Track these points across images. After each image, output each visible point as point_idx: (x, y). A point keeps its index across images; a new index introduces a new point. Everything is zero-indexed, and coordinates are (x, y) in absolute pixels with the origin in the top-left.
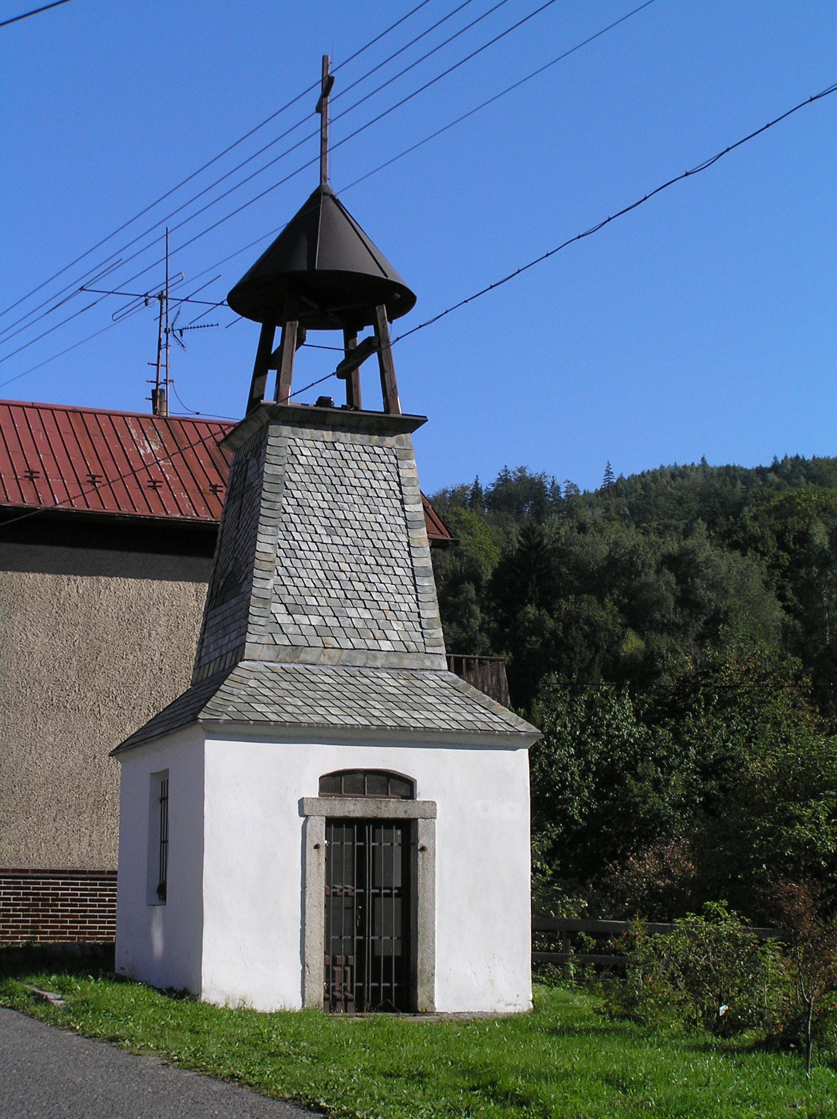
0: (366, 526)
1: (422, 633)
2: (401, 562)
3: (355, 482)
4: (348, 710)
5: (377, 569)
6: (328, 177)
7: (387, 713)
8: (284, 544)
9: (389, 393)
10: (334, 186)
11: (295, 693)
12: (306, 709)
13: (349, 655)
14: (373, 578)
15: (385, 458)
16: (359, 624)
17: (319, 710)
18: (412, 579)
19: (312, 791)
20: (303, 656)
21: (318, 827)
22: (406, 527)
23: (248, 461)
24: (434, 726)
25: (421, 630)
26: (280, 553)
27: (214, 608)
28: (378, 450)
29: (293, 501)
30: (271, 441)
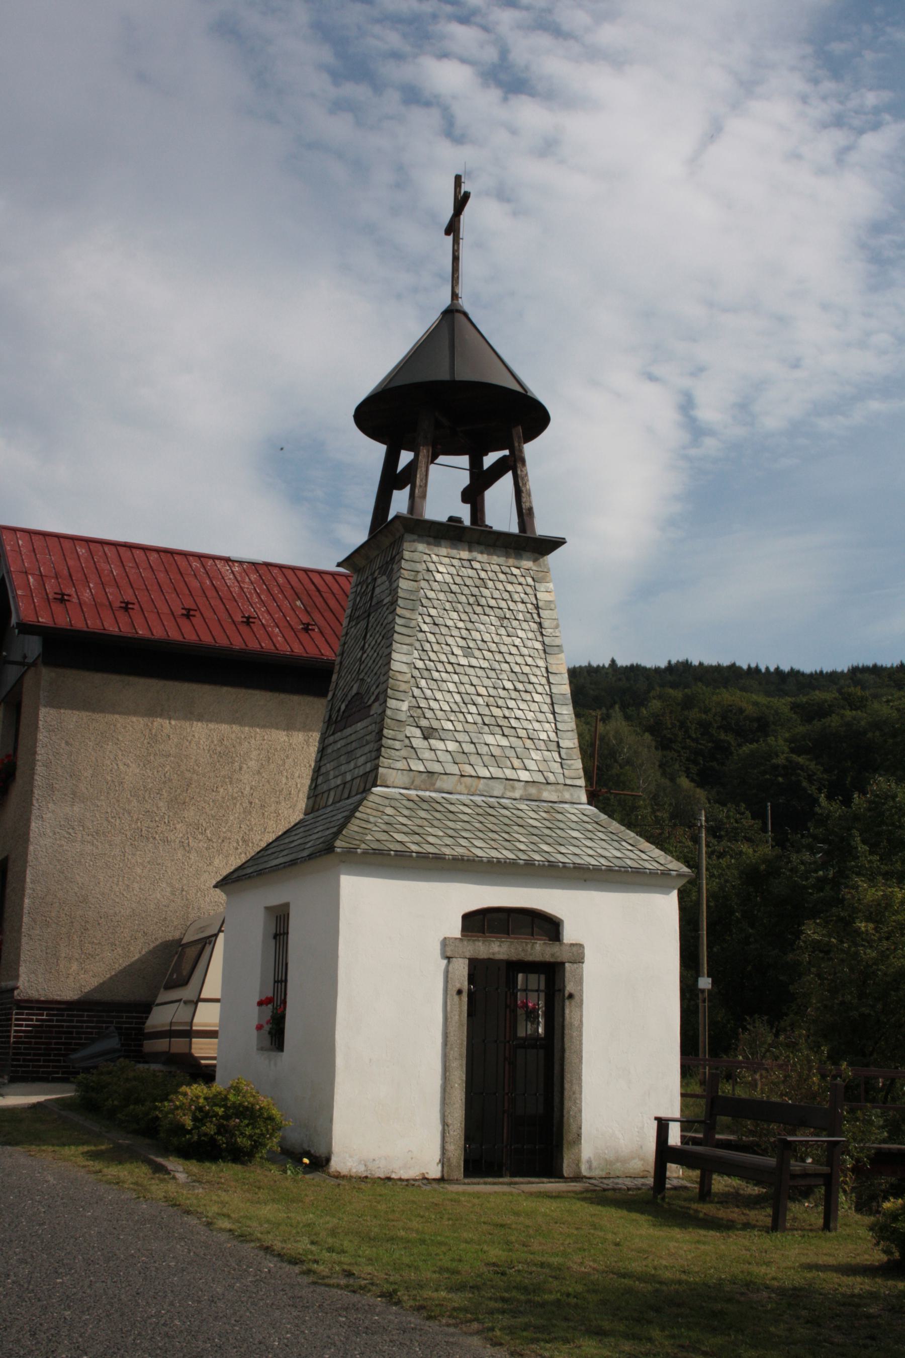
0: (504, 649)
1: (561, 763)
2: (540, 689)
3: (492, 603)
4: (492, 843)
5: (514, 694)
6: (460, 296)
7: (532, 846)
8: (420, 664)
9: (525, 514)
10: (465, 303)
11: (436, 823)
12: (449, 841)
13: (487, 785)
14: (512, 704)
15: (522, 580)
16: (497, 752)
17: (463, 842)
18: (551, 706)
19: (455, 929)
20: (439, 784)
21: (461, 969)
22: (544, 651)
23: (375, 579)
24: (582, 862)
25: (560, 761)
26: (416, 673)
27: (333, 734)
28: (516, 571)
29: (428, 619)
30: (407, 555)
